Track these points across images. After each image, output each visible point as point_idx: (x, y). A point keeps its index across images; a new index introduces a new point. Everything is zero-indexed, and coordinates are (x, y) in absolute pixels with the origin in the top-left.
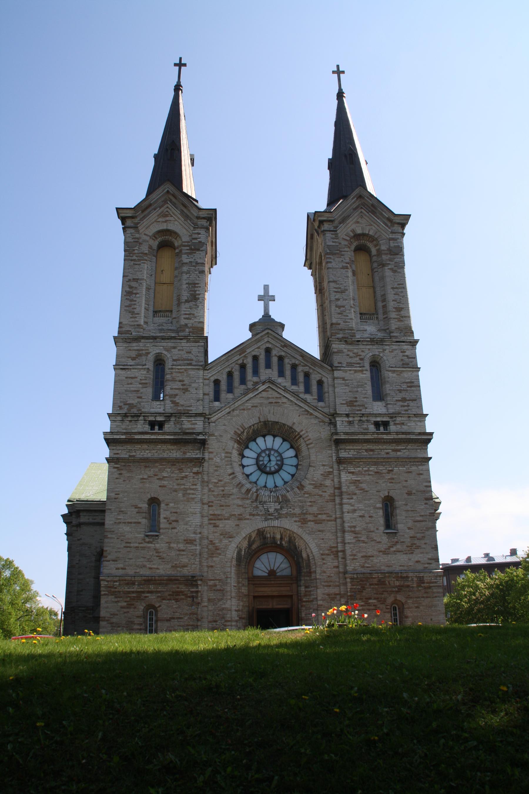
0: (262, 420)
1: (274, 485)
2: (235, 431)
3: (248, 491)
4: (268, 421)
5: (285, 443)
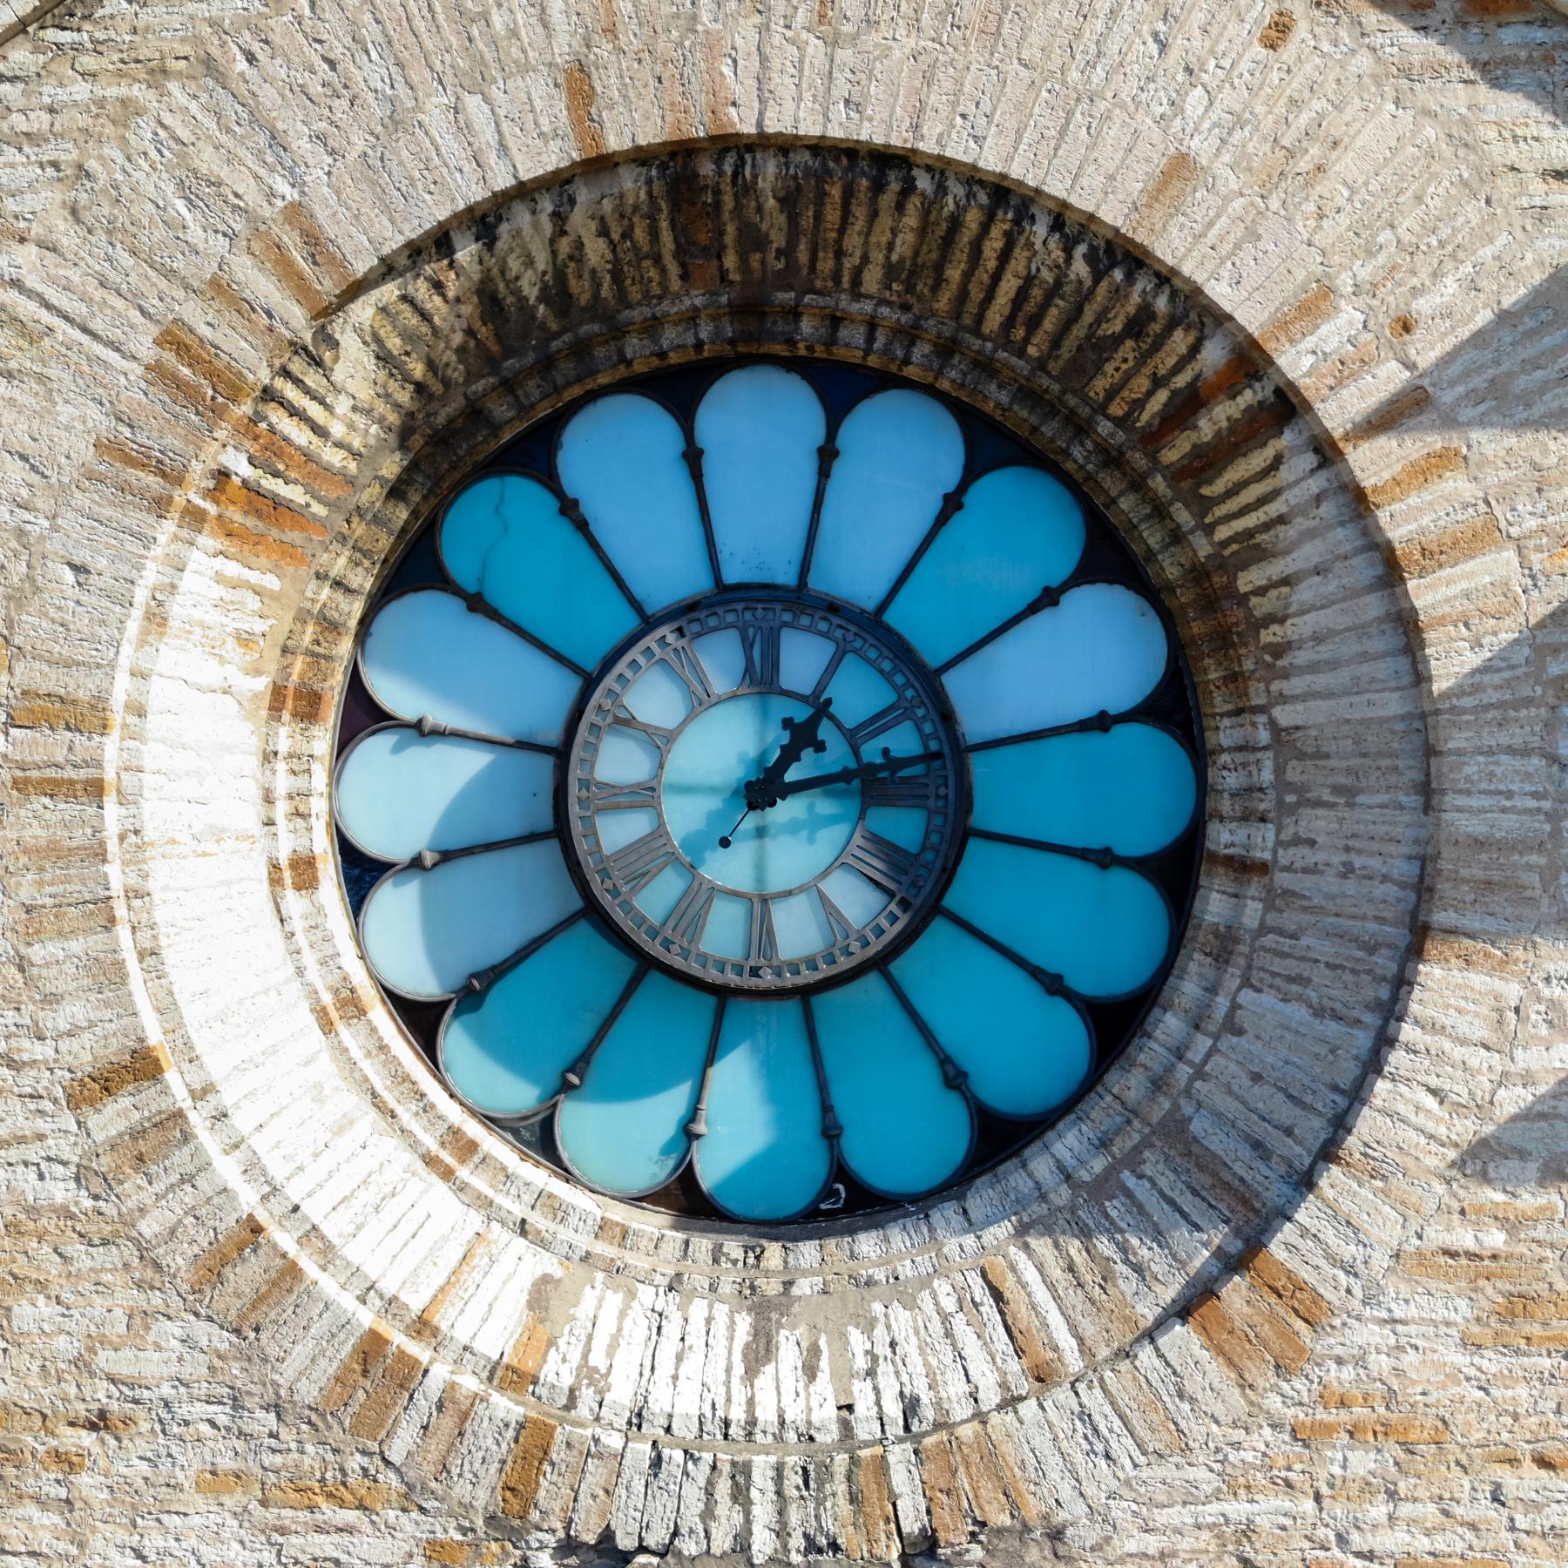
0: (633, 123)
1: (815, 1169)
2: (175, 339)
3: (380, 1372)
4: (727, 145)
5: (1003, 490)
